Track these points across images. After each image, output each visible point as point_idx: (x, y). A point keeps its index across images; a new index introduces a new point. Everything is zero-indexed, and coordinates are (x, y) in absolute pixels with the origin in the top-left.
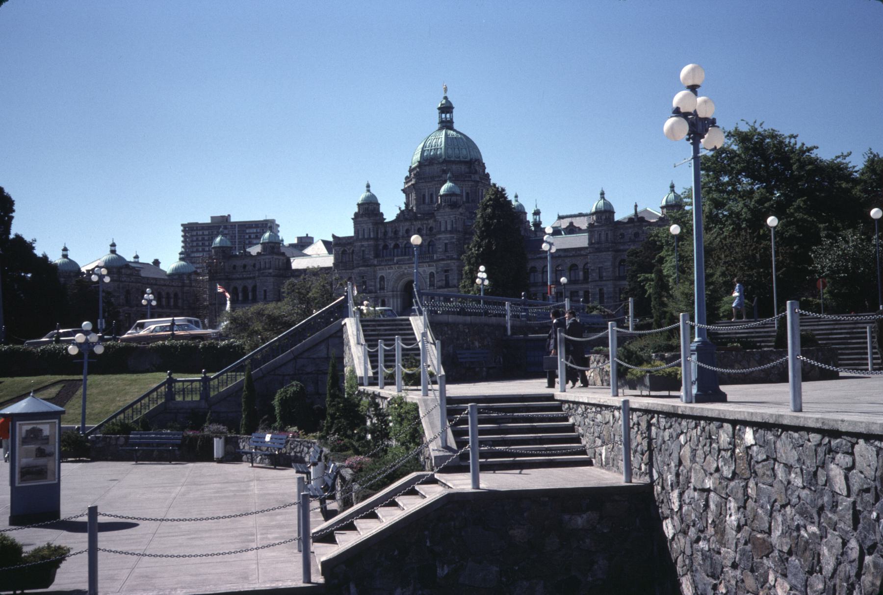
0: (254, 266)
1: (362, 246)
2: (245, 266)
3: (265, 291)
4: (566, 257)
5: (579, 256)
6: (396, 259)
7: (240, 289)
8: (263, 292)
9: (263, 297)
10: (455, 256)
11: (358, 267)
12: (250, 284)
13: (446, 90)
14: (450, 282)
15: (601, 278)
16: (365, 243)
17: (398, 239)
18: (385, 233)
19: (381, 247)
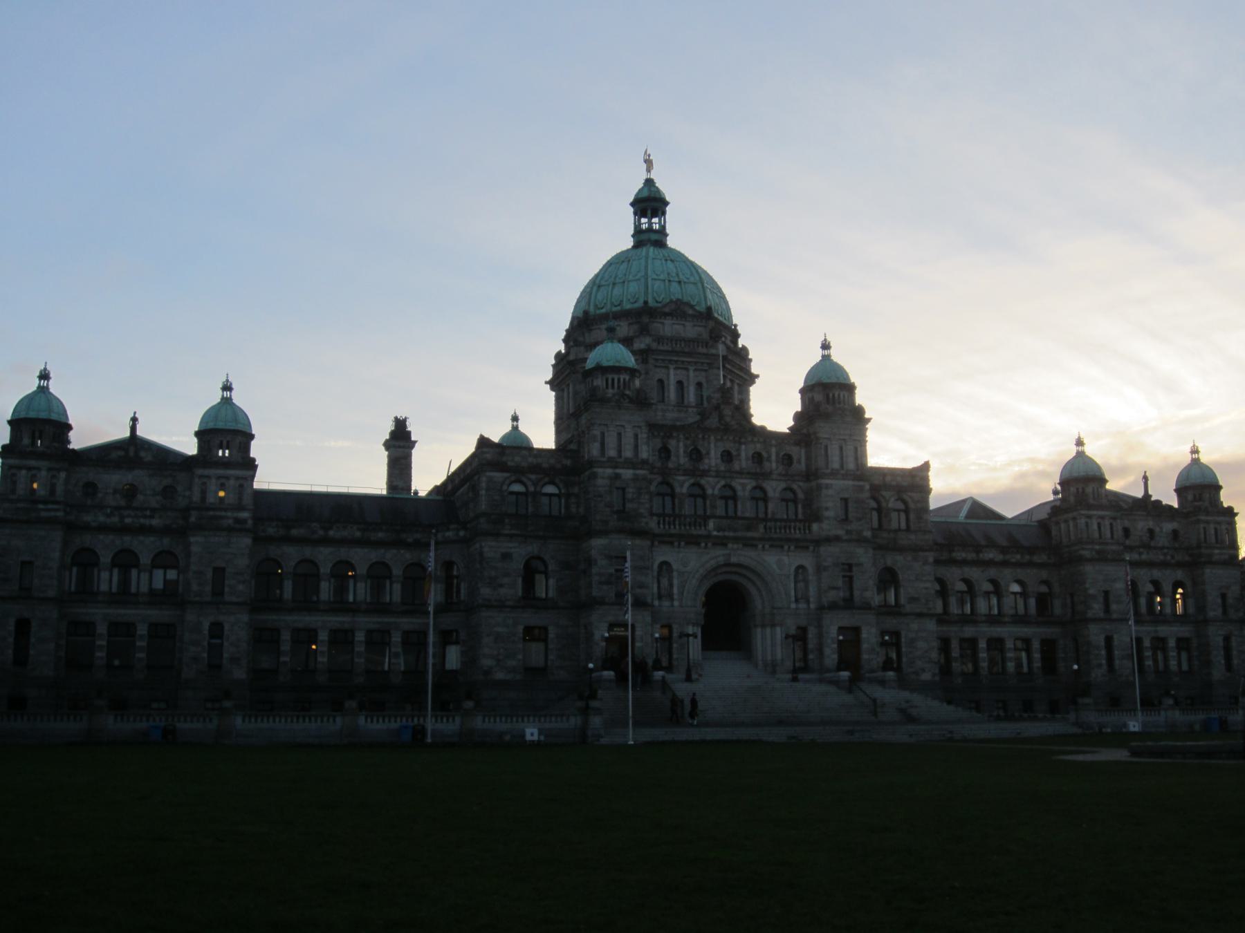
0: (169, 492)
1: (617, 476)
2: (131, 492)
3: (219, 572)
4: (1005, 564)
5: (1031, 564)
6: (711, 524)
7: (106, 558)
8: (209, 575)
9: (208, 589)
10: (868, 534)
11: (604, 533)
12: (145, 548)
13: (649, 163)
14: (857, 593)
15: (1107, 609)
16: (627, 473)
17: (704, 473)
18: (665, 452)
19: (652, 488)
